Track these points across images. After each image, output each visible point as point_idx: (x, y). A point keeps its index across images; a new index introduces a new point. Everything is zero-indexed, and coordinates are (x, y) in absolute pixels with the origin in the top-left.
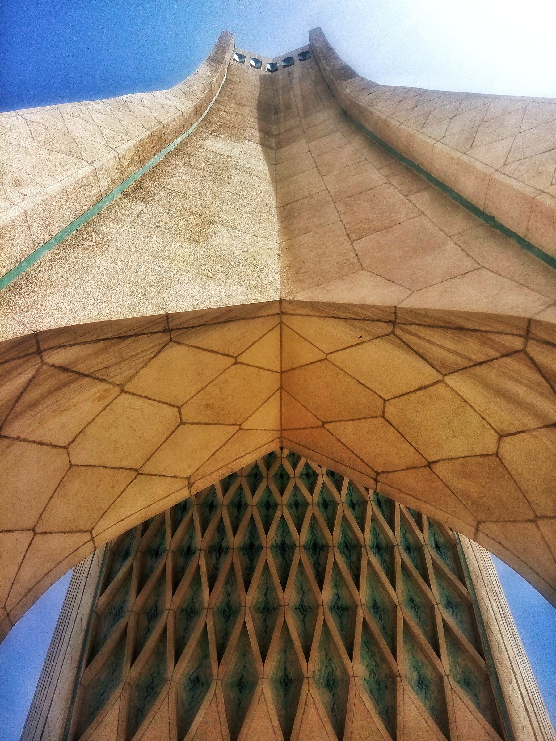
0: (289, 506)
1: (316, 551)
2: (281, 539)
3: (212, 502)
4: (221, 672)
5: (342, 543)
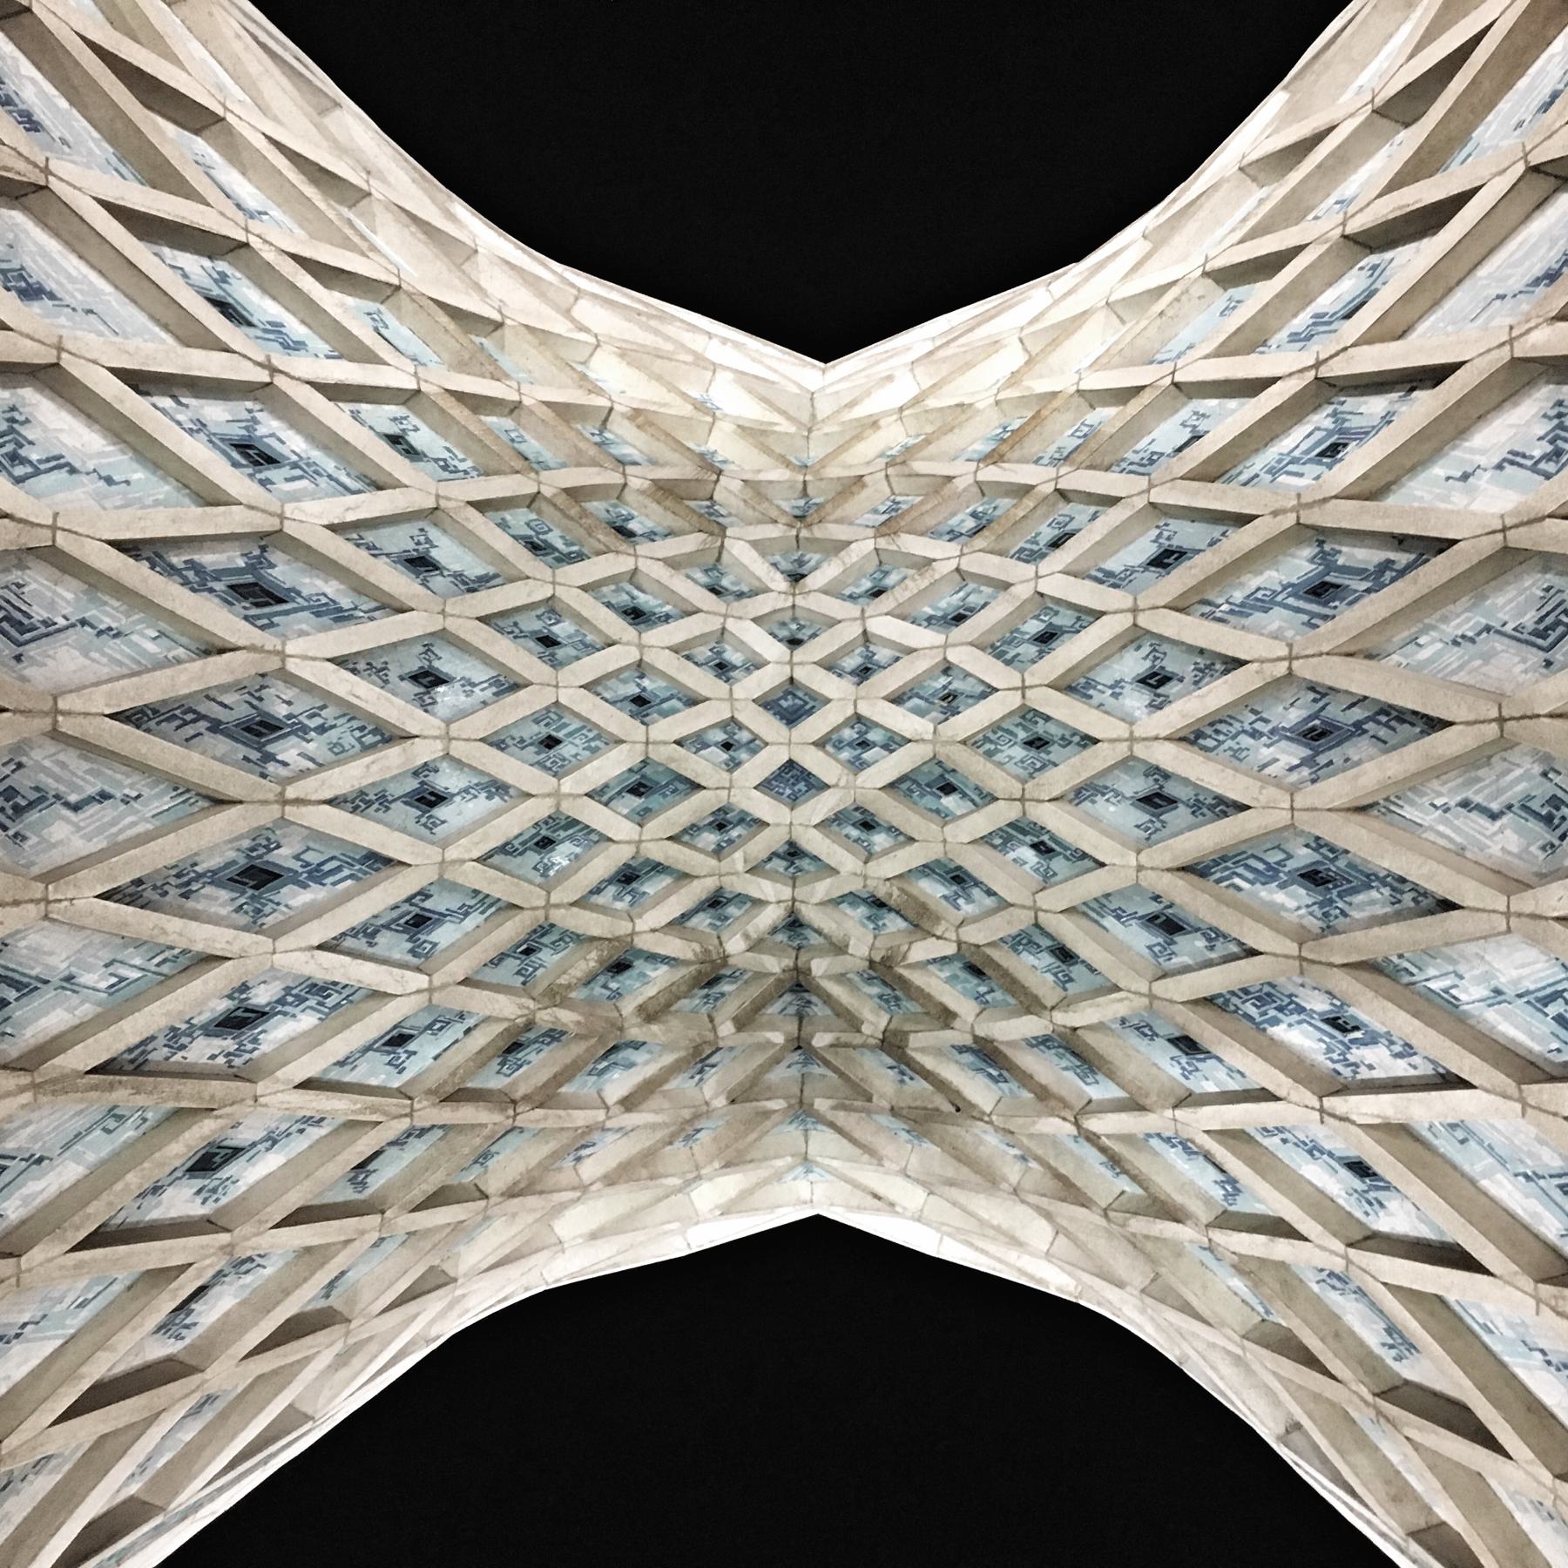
1: (1338, 586)
2: (1284, 743)
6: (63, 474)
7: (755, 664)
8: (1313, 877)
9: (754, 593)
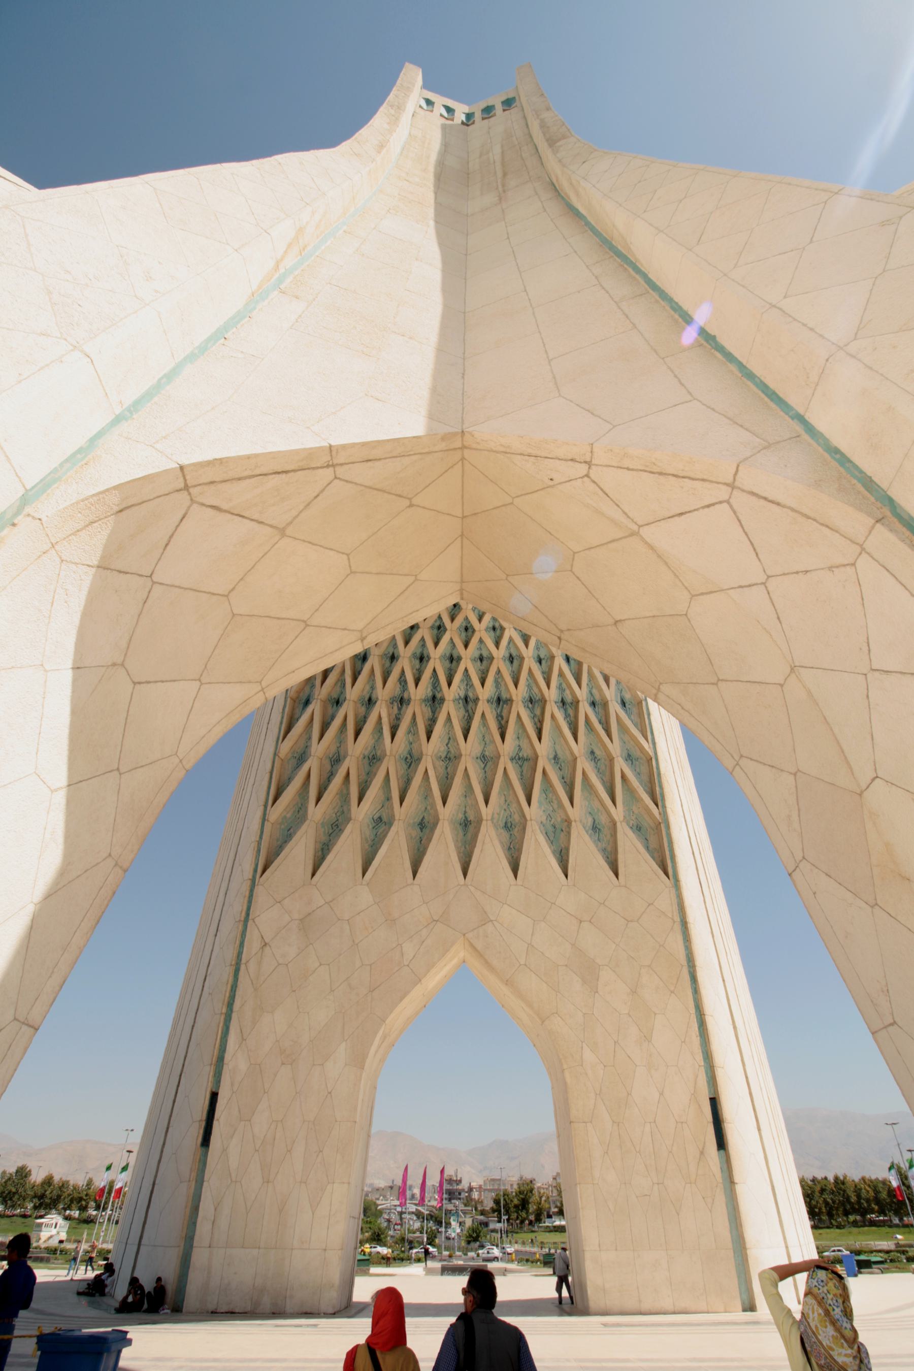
0: (474, 660)
3: (393, 654)
4: (404, 815)
8: (434, 698)
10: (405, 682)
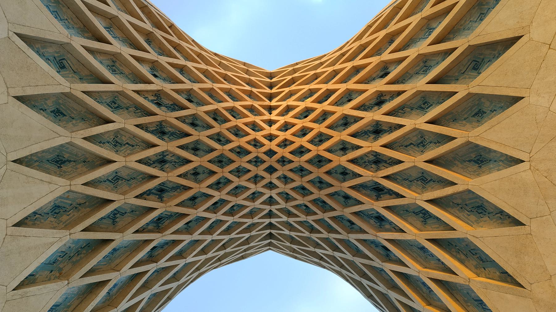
0: (195, 168)
5: (162, 215)
6: (416, 211)
7: (279, 178)
8: (164, 133)
9: (279, 193)
10: (174, 110)
